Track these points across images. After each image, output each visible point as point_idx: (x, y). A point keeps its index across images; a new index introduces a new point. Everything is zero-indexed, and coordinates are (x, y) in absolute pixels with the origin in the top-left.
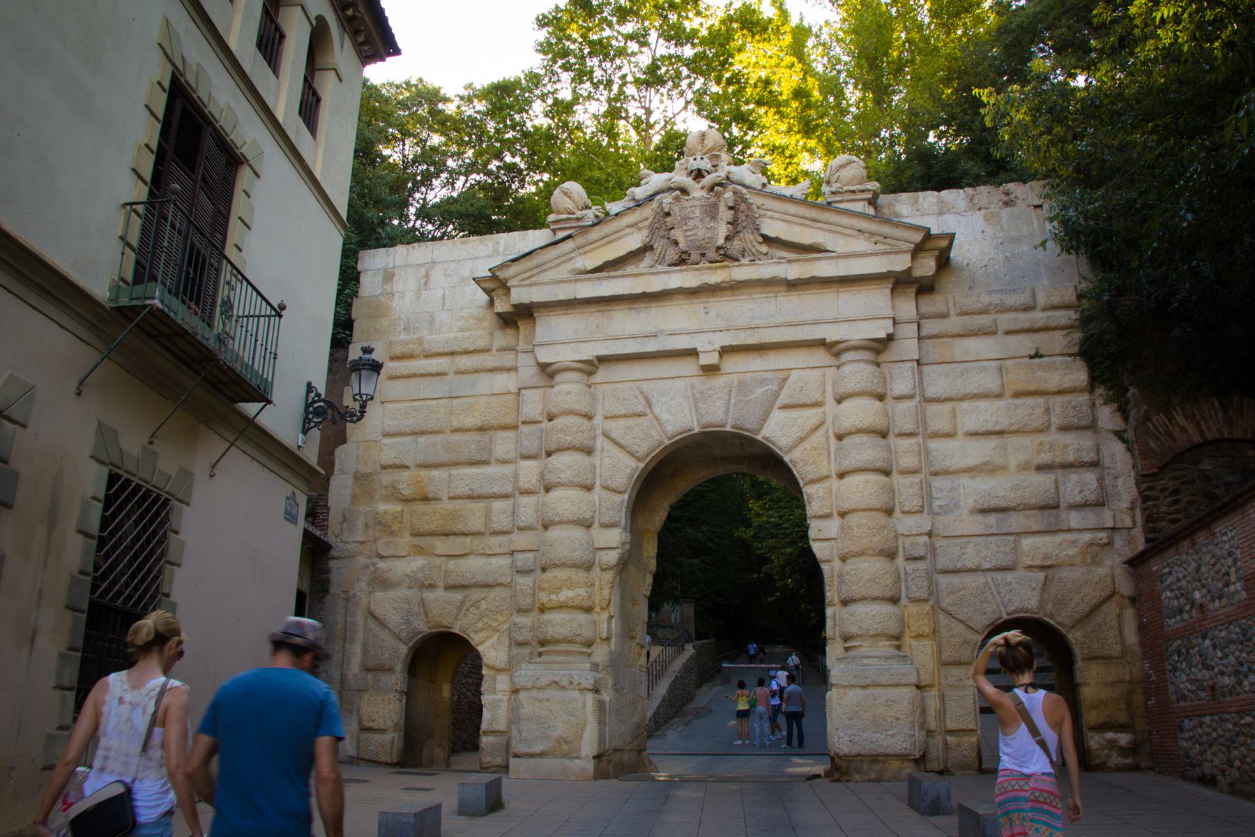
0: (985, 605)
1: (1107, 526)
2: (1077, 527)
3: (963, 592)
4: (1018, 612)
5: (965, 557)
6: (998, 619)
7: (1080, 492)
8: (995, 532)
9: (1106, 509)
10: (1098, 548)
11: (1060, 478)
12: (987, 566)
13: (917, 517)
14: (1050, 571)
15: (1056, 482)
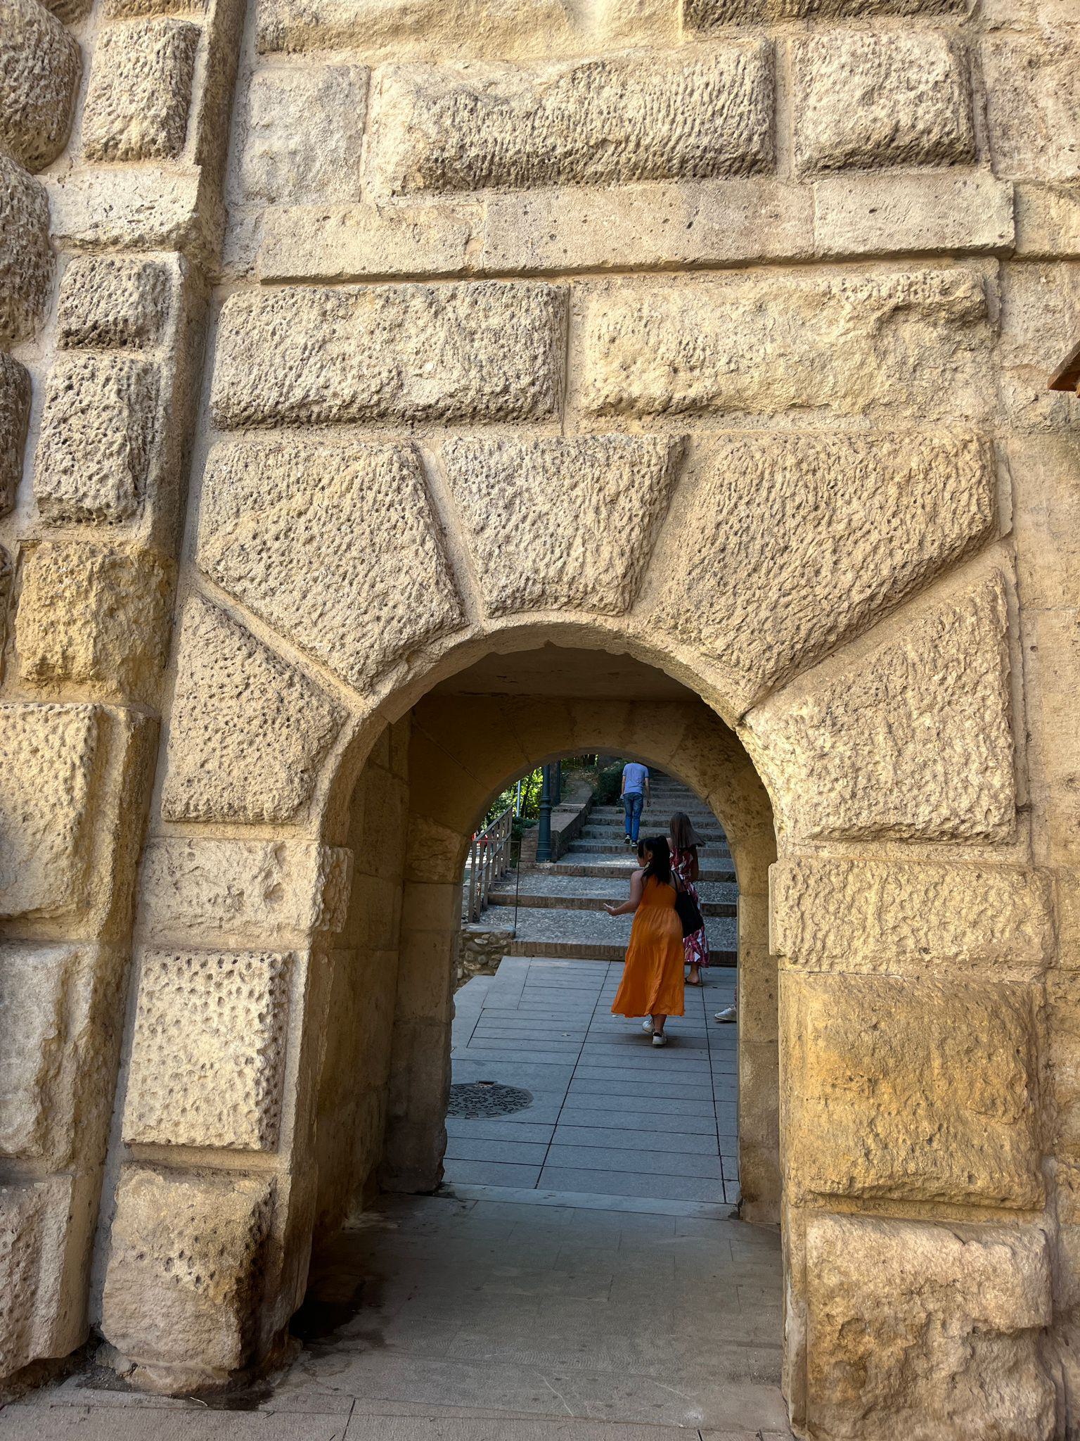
0: (388, 561)
1: (978, 241)
2: (841, 243)
3: (299, 501)
4: (538, 602)
5: (334, 349)
6: (440, 629)
7: (868, 97)
8: (480, 261)
9: (982, 173)
10: (931, 335)
11: (789, 50)
12: (425, 392)
13: (148, 173)
14: (701, 432)
15: (770, 57)
